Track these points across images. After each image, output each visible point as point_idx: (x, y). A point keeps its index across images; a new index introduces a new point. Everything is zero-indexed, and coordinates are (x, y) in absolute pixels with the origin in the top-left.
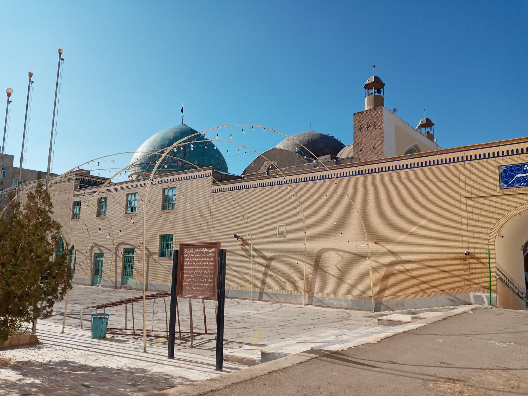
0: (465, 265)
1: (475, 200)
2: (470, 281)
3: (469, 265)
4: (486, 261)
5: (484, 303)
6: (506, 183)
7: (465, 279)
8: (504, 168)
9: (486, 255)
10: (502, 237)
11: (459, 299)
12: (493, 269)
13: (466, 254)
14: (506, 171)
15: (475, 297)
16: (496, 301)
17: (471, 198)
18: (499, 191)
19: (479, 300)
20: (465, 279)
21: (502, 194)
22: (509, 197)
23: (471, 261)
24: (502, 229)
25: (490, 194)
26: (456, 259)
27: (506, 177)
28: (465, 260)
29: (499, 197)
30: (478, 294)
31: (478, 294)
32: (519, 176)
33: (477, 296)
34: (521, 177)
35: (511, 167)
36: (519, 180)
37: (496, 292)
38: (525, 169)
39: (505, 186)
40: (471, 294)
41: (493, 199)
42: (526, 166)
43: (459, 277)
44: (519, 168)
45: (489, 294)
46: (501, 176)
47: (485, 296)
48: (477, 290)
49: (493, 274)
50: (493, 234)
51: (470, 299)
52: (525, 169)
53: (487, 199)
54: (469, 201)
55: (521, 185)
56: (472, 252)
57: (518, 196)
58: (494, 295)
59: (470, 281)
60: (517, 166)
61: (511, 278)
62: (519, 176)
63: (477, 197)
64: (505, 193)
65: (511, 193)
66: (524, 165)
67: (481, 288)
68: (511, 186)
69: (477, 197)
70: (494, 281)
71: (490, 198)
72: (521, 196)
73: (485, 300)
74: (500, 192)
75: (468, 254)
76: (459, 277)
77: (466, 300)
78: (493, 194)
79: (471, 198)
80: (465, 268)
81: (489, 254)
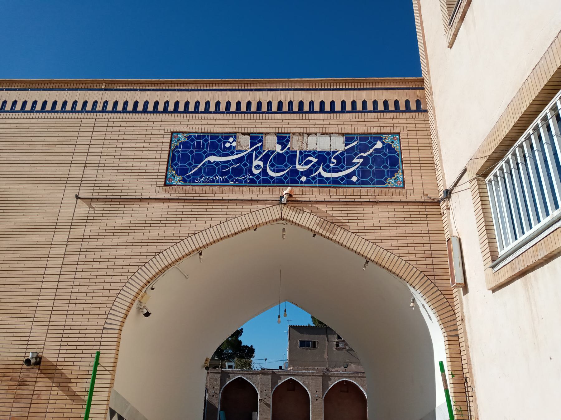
0: (17, 399)
1: (99, 208)
4: (81, 387)
6: (182, 172)
8: (183, 139)
10: (147, 314)
13: (28, 362)
14: (186, 145)
17: (90, 201)
18: (161, 189)
21: (167, 196)
24: (150, 292)
25: (138, 196)
27: (185, 158)
28: (22, 383)
29: (158, 206)
32: (212, 159)
34: (217, 164)
35: (199, 137)
36: (211, 169)
38: (228, 145)
39: (178, 178)
42: (231, 140)
44: (217, 142)
46: (173, 155)
50: (121, 305)
52: (228, 145)
53: (129, 208)
54: (83, 207)
55: (213, 181)
56: (50, 356)
57: (203, 206)
60: (212, 138)
62: (212, 159)
63: (105, 200)
64: (174, 196)
65: (189, 196)
66: (227, 138)
68: (188, 180)
69: (105, 200)
71: (136, 206)
72: (210, 206)
74: (162, 192)
75: (36, 362)
78: (146, 195)
79: (90, 201)
81: (97, 363)
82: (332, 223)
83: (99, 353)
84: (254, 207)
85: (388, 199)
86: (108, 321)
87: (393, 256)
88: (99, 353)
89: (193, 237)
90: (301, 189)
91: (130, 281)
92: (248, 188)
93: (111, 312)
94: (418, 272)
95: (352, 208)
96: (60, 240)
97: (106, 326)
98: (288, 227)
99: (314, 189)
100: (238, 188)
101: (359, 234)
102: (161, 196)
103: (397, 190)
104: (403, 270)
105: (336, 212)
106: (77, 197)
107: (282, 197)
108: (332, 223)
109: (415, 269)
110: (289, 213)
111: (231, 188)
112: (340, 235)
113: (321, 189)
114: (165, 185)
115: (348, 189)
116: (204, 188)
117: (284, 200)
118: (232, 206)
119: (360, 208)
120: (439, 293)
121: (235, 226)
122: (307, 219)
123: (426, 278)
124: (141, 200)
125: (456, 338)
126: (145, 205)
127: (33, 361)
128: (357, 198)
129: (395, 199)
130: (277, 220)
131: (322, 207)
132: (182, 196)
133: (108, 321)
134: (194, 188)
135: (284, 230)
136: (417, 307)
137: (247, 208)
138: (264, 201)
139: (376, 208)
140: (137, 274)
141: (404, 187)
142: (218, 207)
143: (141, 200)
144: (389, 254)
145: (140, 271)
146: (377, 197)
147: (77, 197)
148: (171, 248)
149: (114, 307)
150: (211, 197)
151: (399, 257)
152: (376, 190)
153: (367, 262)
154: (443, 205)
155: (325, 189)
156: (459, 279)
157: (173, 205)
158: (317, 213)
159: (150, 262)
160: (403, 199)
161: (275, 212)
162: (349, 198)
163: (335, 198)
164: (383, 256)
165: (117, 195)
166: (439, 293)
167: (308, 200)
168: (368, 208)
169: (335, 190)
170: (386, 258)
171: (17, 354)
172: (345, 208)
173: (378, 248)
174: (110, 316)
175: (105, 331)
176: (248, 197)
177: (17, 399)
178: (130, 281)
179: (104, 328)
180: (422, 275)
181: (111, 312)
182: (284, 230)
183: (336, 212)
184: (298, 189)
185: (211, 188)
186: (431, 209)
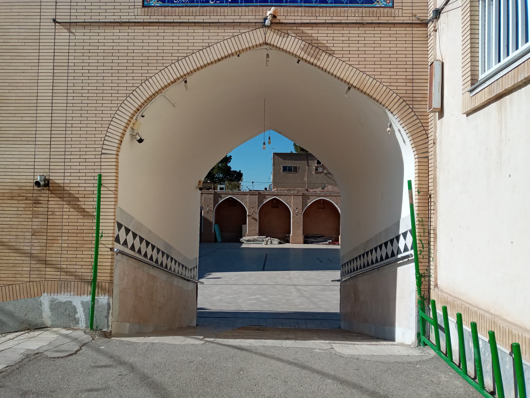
0: (35, 215)
1: (79, 32)
2: (45, 262)
3: (49, 214)
4: (90, 205)
5: (77, 321)
7: (31, 256)
9: (92, 186)
10: (141, 141)
11: (11, 315)
12: (108, 227)
13: (37, 184)
15: (55, 306)
16: (107, 317)
17: (69, 25)
18: (140, 10)
19: (65, 316)
20: (31, 256)
21: (147, 19)
22: (161, 30)
23: (54, 203)
24: (140, 119)
25: (117, 19)
26: (12, 198)
28: (37, 202)
29: (139, 30)
30: (63, 298)
31: (63, 298)
33: (60, 303)
37: (110, 292)
40: (45, 300)
41: (123, 33)
43: (17, 250)
45: (89, 298)
47: (79, 301)
48: (62, 286)
49: (107, 241)
50: (115, 131)
51: (41, 316)
54: (63, 34)
56: (56, 178)
57: (184, 30)
58: (103, 299)
59: (45, 262)
61: (167, 245)
63: (85, 24)
64: (154, 19)
65: (169, 19)
67: (69, 280)
69: (85, 24)
70: (105, 261)
71: (116, 30)
73: (81, 314)
74: (141, 15)
75: (46, 184)
76: (17, 250)
77: (31, 317)
78: (125, 19)
79: (69, 25)
80: (36, 224)
81: (100, 185)
82: (317, 47)
83: (100, 176)
84: (236, 31)
85: (375, 20)
86: (104, 147)
87: (375, 81)
88: (100, 176)
89: (177, 64)
90: (286, 9)
91: (120, 109)
92: (230, 9)
93: (107, 138)
94: (398, 98)
95: (338, 31)
96: (46, 67)
97: (104, 151)
98: (272, 53)
99: (300, 9)
100: (219, 9)
101: (343, 59)
102: (140, 19)
103: (386, 10)
104: (384, 96)
105: (322, 35)
106: (55, 21)
107: (265, 19)
108: (317, 47)
109: (395, 95)
110: (273, 38)
111: (212, 8)
112: (324, 61)
113: (307, 9)
114: (143, 6)
115: (335, 9)
116: (184, 9)
117: (267, 22)
118: (213, 30)
119: (346, 31)
120: (415, 117)
121: (218, 52)
122: (291, 44)
123: (404, 103)
124: (121, 24)
125: (426, 160)
126: (125, 29)
127: (42, 183)
128: (344, 20)
129: (383, 20)
130: (260, 45)
131: (308, 30)
132: (162, 19)
133: (104, 147)
134: (174, 9)
135: (268, 56)
136: (393, 131)
137: (229, 32)
138: (247, 24)
139: (362, 30)
140: (126, 102)
141: (393, 7)
142: (199, 30)
143: (121, 24)
144: (371, 79)
145: (128, 99)
146: (365, 18)
147: (55, 21)
148: (157, 76)
149: (108, 134)
150: (192, 19)
151: (381, 82)
152: (364, 9)
153: (349, 88)
154: (431, 26)
155: (311, 9)
156: (436, 104)
157: (154, 29)
158: (301, 36)
159: (138, 90)
160: (391, 20)
161: (258, 36)
162: (336, 19)
163: (321, 19)
164: (365, 82)
165: (95, 19)
166: (415, 117)
167: (293, 21)
168: (354, 31)
169: (321, 10)
170: (368, 84)
171: (27, 178)
172: (330, 31)
173: (361, 73)
174: (105, 142)
175: (103, 156)
176: (229, 19)
177: (35, 215)
178: (120, 109)
179: (102, 154)
180: (401, 100)
181: (107, 138)
182: (268, 56)
183: (322, 35)
184: (282, 9)
185: (191, 9)
186: (418, 31)
